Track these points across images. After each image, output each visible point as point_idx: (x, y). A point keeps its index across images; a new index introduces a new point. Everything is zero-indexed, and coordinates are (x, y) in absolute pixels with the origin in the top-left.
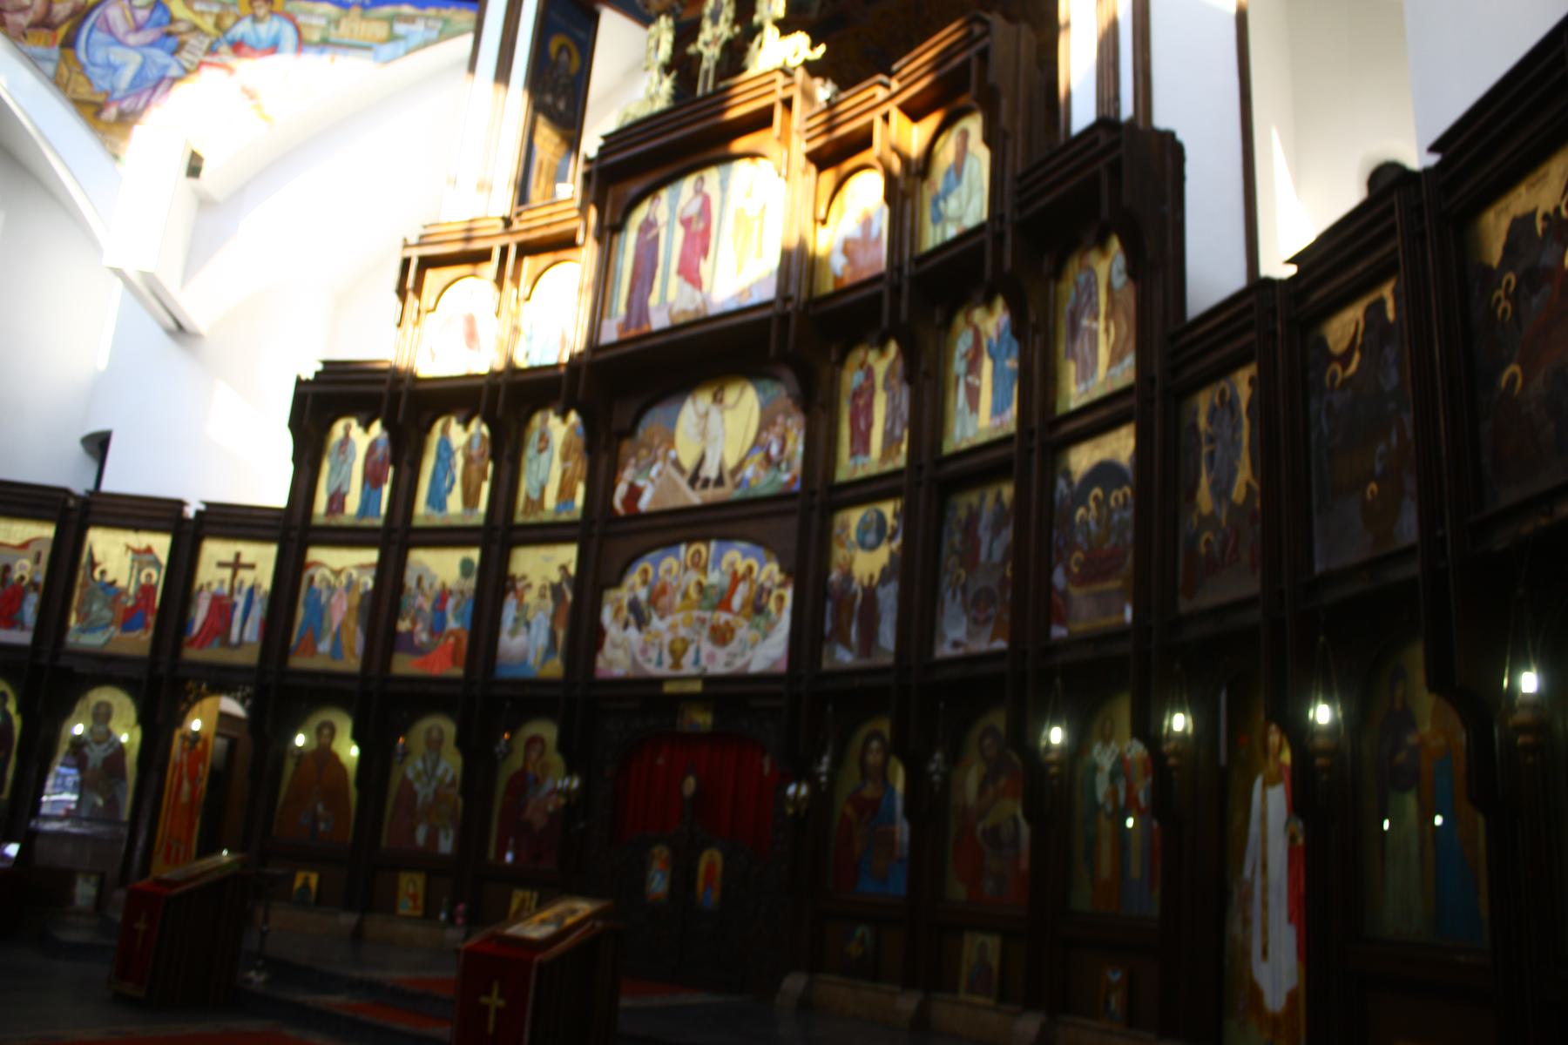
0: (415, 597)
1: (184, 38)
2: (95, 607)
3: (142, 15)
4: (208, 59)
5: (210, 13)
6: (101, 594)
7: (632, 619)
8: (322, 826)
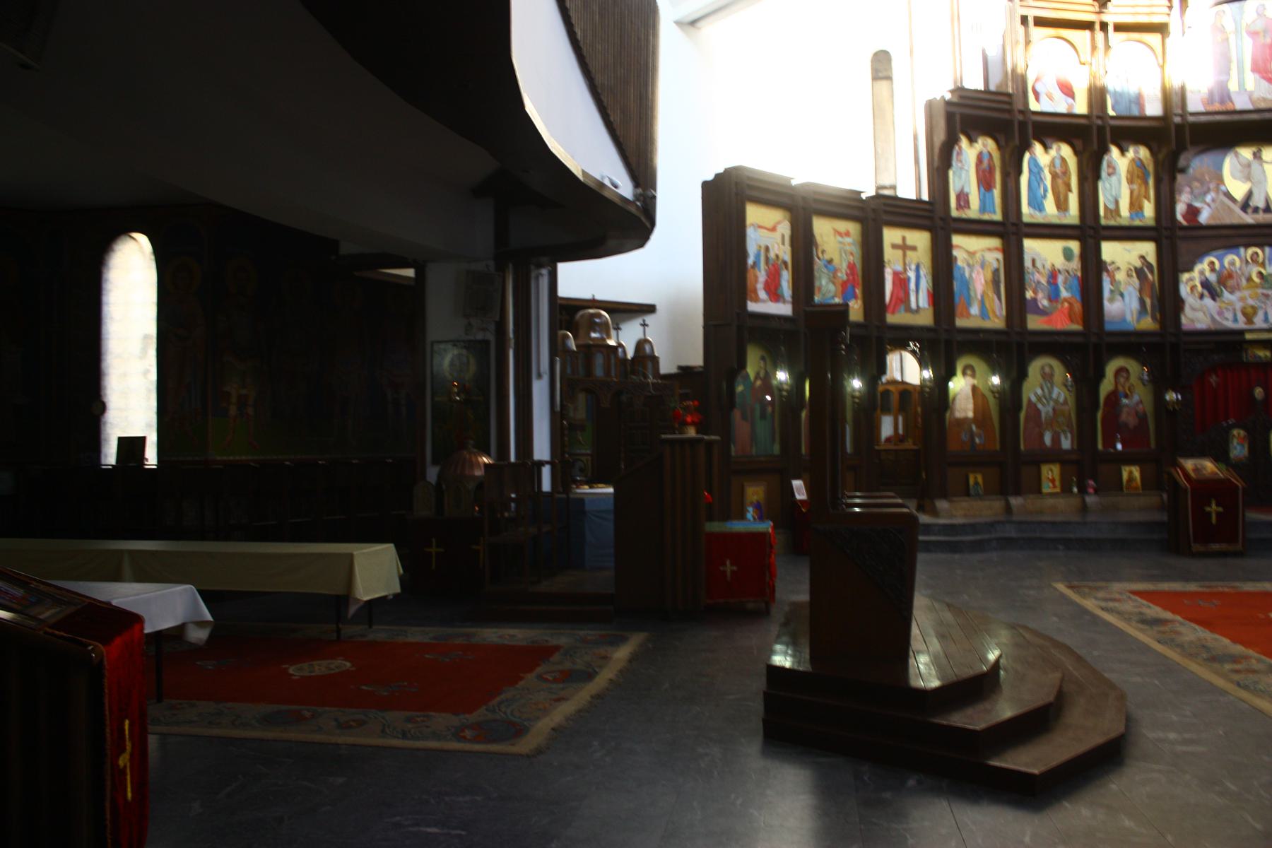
0: (1033, 274)
2: (824, 282)
6: (824, 270)
7: (1206, 293)
8: (977, 440)
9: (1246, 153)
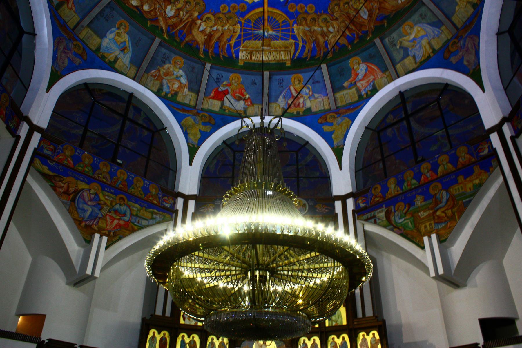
1: (103, 206)
3: (92, 196)
4: (108, 214)
5: (109, 200)
9: (261, 342)
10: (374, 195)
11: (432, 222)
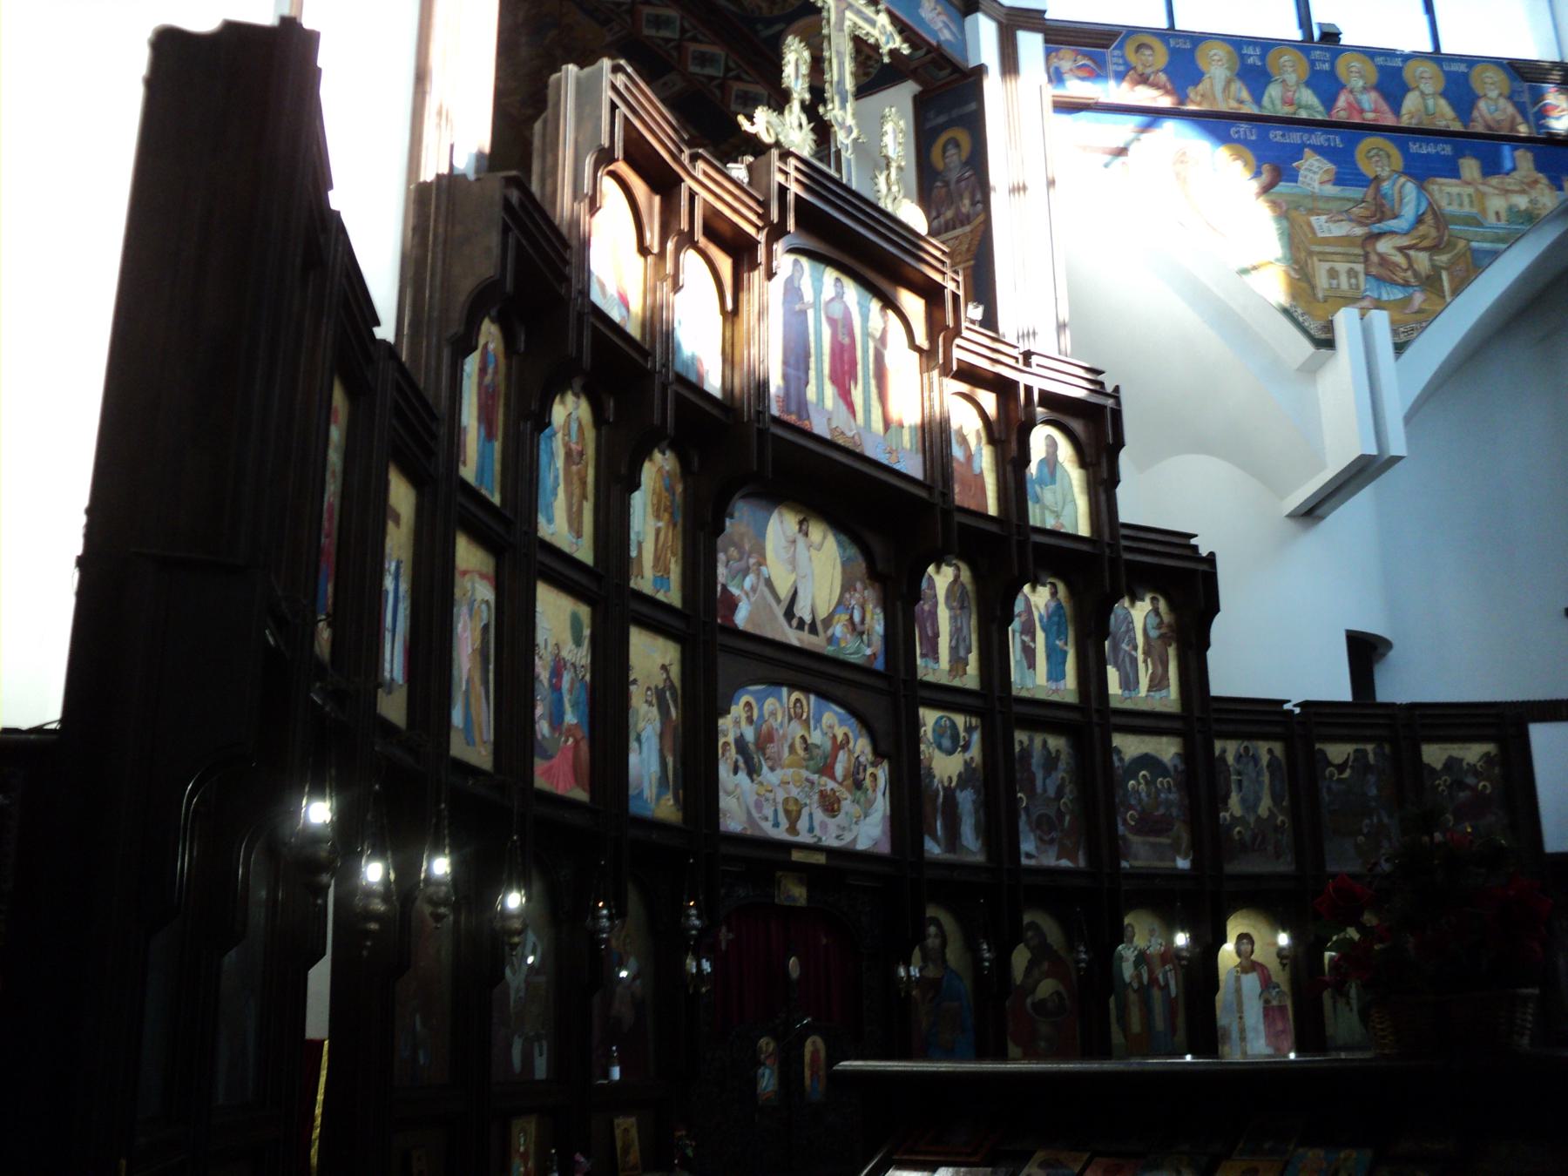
7: (741, 764)
10: (1134, 68)
11: (1359, 268)
